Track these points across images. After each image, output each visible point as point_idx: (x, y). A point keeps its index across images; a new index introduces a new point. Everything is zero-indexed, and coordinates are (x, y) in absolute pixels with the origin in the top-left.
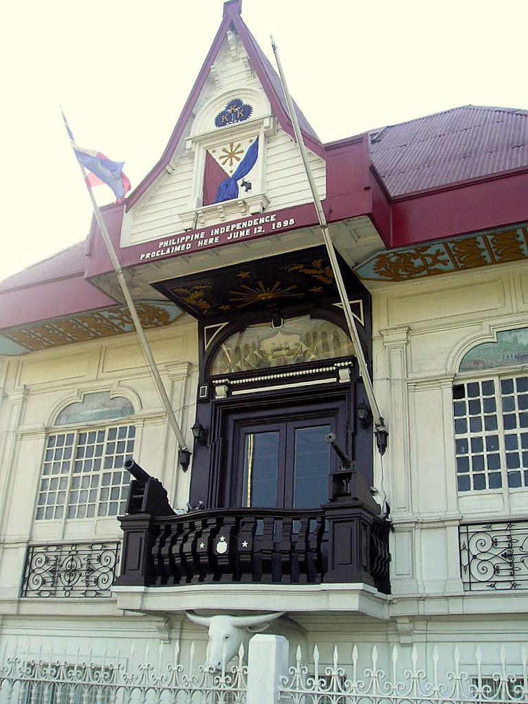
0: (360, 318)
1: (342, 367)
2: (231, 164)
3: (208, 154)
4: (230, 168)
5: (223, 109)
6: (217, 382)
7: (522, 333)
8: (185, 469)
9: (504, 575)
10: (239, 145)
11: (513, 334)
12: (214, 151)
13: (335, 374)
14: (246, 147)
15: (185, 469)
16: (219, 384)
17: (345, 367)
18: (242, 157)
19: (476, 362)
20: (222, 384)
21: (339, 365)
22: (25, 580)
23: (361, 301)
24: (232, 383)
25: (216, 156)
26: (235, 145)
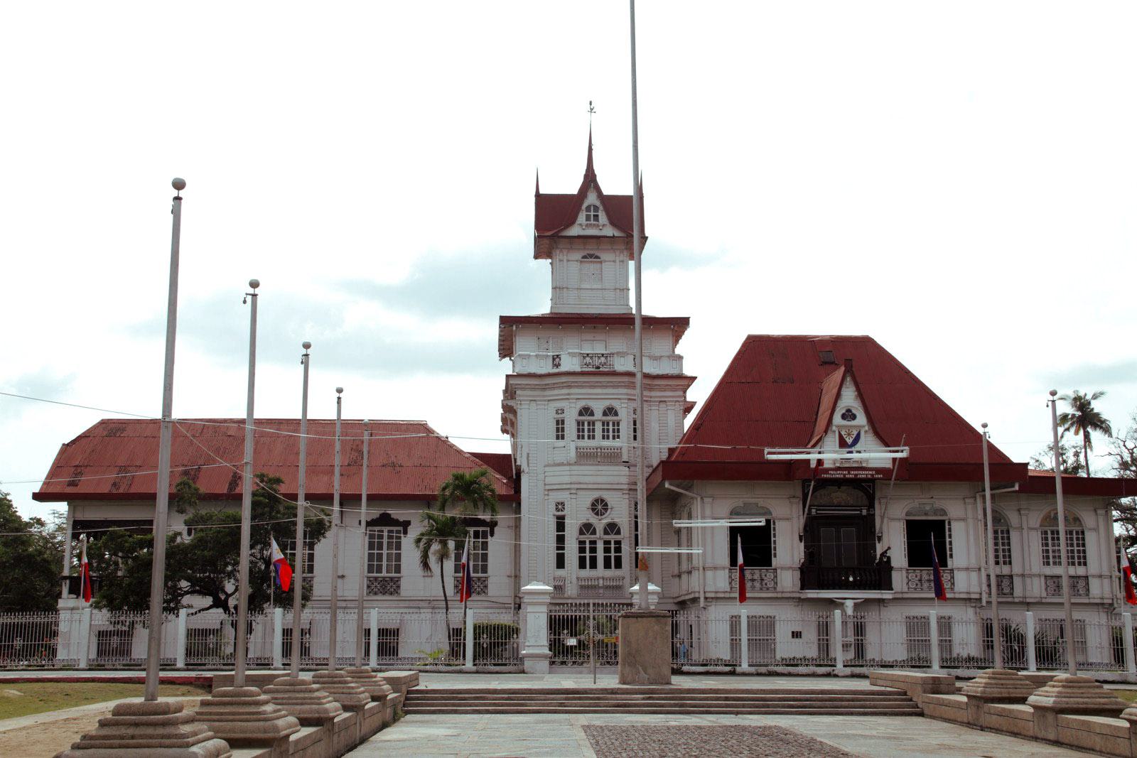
3: (839, 432)
4: (849, 441)
5: (844, 411)
8: (801, 542)
9: (919, 586)
13: (861, 510)
14: (855, 433)
15: (801, 542)
18: (854, 436)
19: (911, 513)
22: (730, 583)
25: (843, 433)
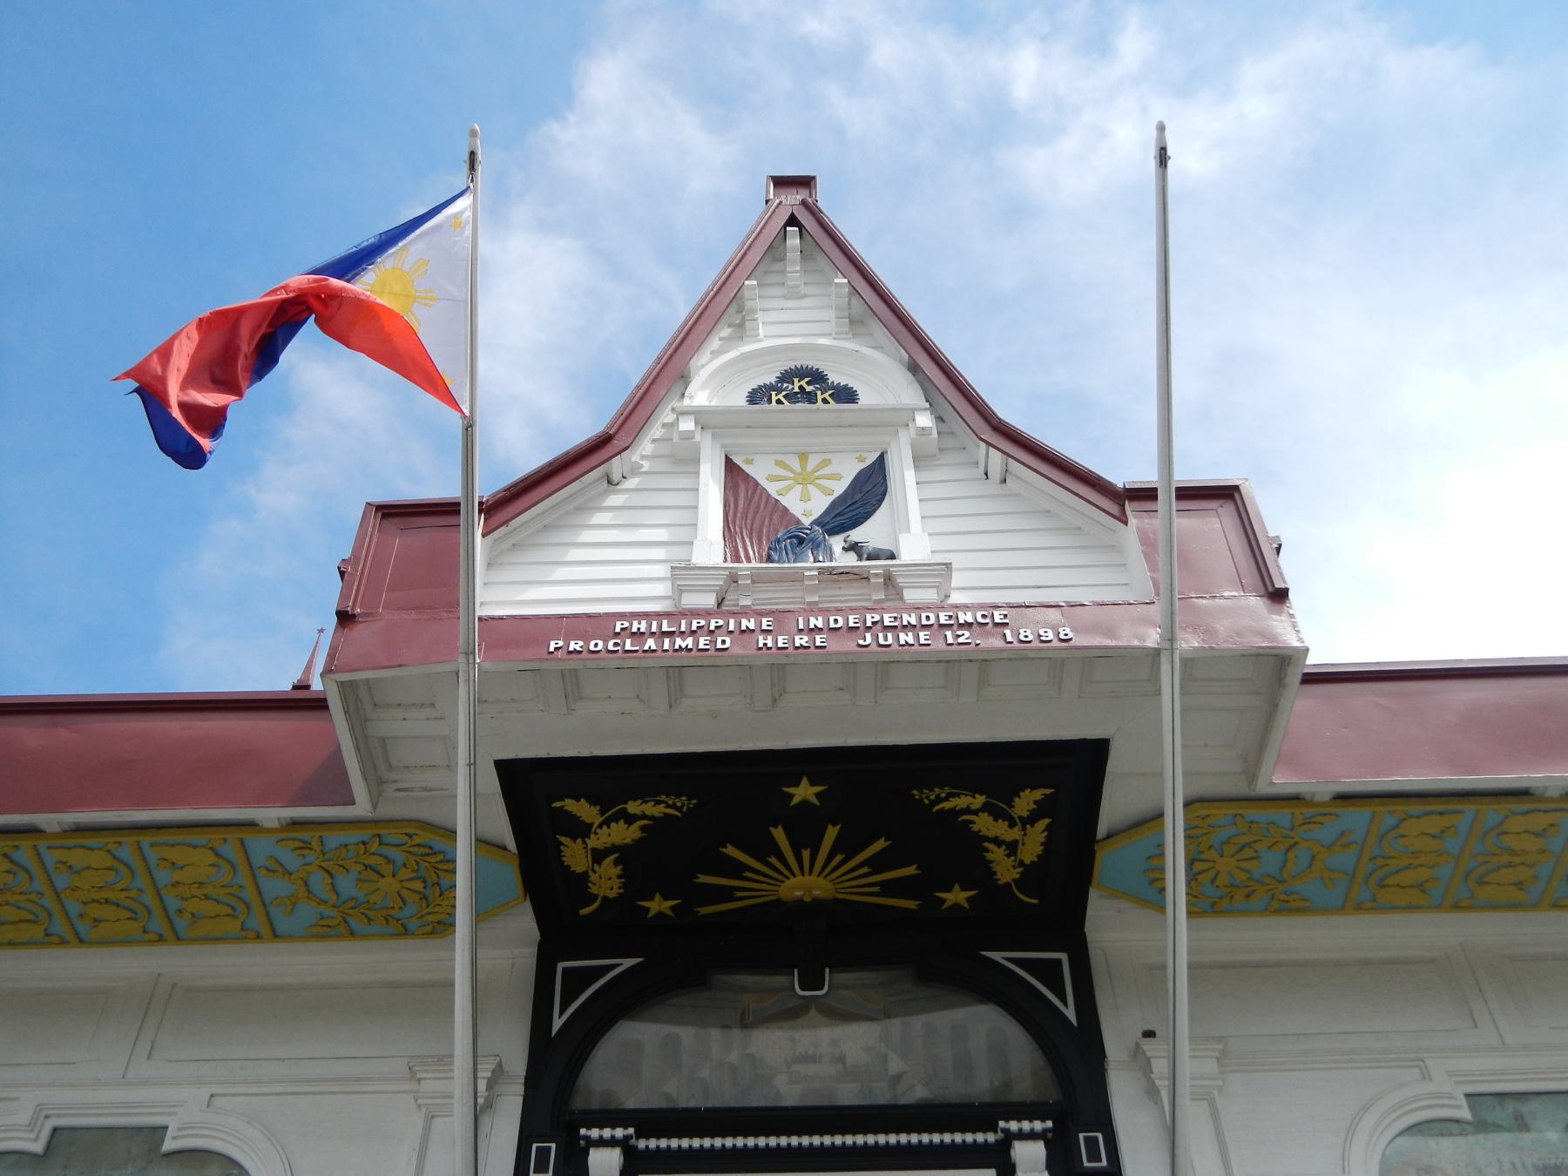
0: (1064, 1001)
1: (1022, 1136)
2: (805, 498)
6: (595, 1133)
7: (1535, 1105)
10: (827, 463)
11: (1511, 1106)
12: (749, 462)
16: (601, 1143)
17: (1032, 1136)
18: (840, 488)
20: (611, 1143)
21: (1013, 1126)
23: (1063, 956)
24: (642, 1144)
25: (759, 470)
26: (813, 462)
